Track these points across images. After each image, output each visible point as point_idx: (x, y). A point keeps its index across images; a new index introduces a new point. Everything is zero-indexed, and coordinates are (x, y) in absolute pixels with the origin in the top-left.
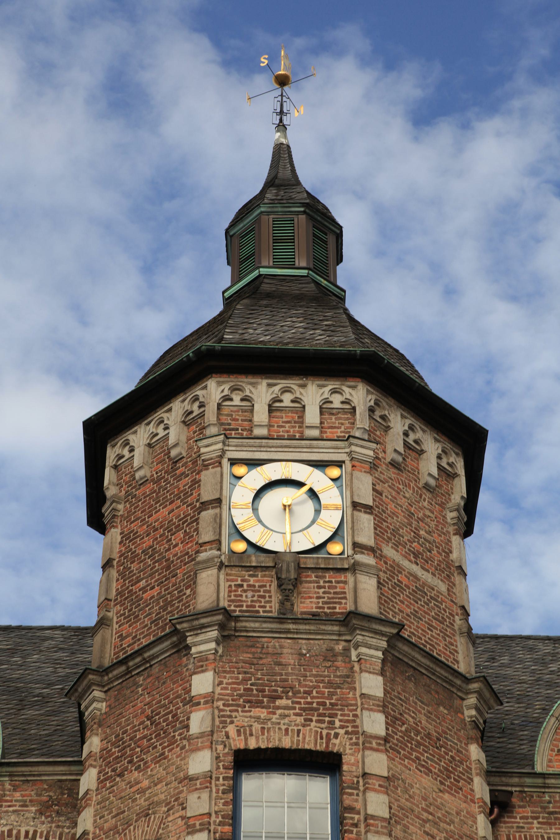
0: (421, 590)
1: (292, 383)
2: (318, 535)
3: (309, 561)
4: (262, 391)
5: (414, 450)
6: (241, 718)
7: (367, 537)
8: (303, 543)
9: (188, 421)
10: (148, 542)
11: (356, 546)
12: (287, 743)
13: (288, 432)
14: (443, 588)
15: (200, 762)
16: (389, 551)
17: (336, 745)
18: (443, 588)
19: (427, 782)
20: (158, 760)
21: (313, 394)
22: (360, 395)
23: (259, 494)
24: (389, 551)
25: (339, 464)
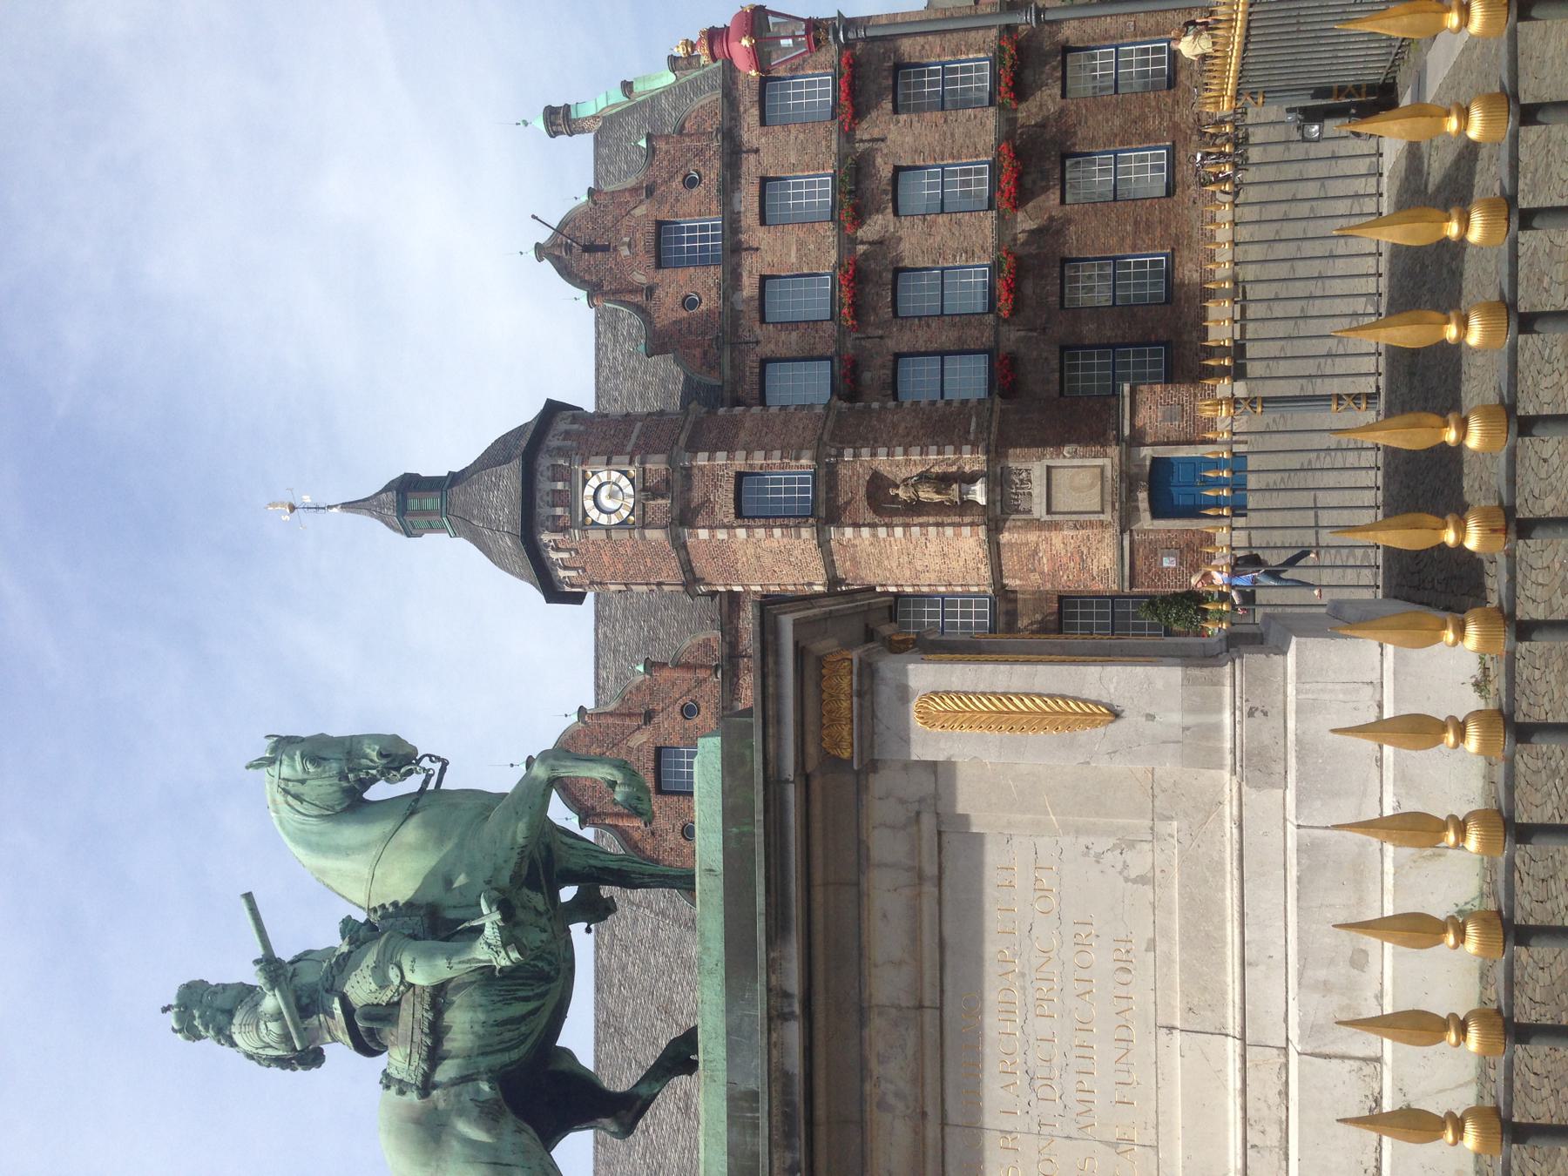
0: (642, 434)
1: (538, 495)
2: (624, 482)
3: (639, 486)
4: (543, 510)
5: (567, 434)
6: (720, 516)
7: (626, 459)
8: (629, 490)
9: (557, 549)
10: (620, 566)
11: (631, 463)
12: (731, 496)
13: (568, 500)
14: (639, 424)
15: (741, 533)
16: (629, 449)
17: (732, 474)
18: (639, 424)
19: (742, 435)
20: (734, 552)
21: (544, 485)
22: (544, 462)
23: (602, 511)
24: (629, 449)
25: (584, 472)
